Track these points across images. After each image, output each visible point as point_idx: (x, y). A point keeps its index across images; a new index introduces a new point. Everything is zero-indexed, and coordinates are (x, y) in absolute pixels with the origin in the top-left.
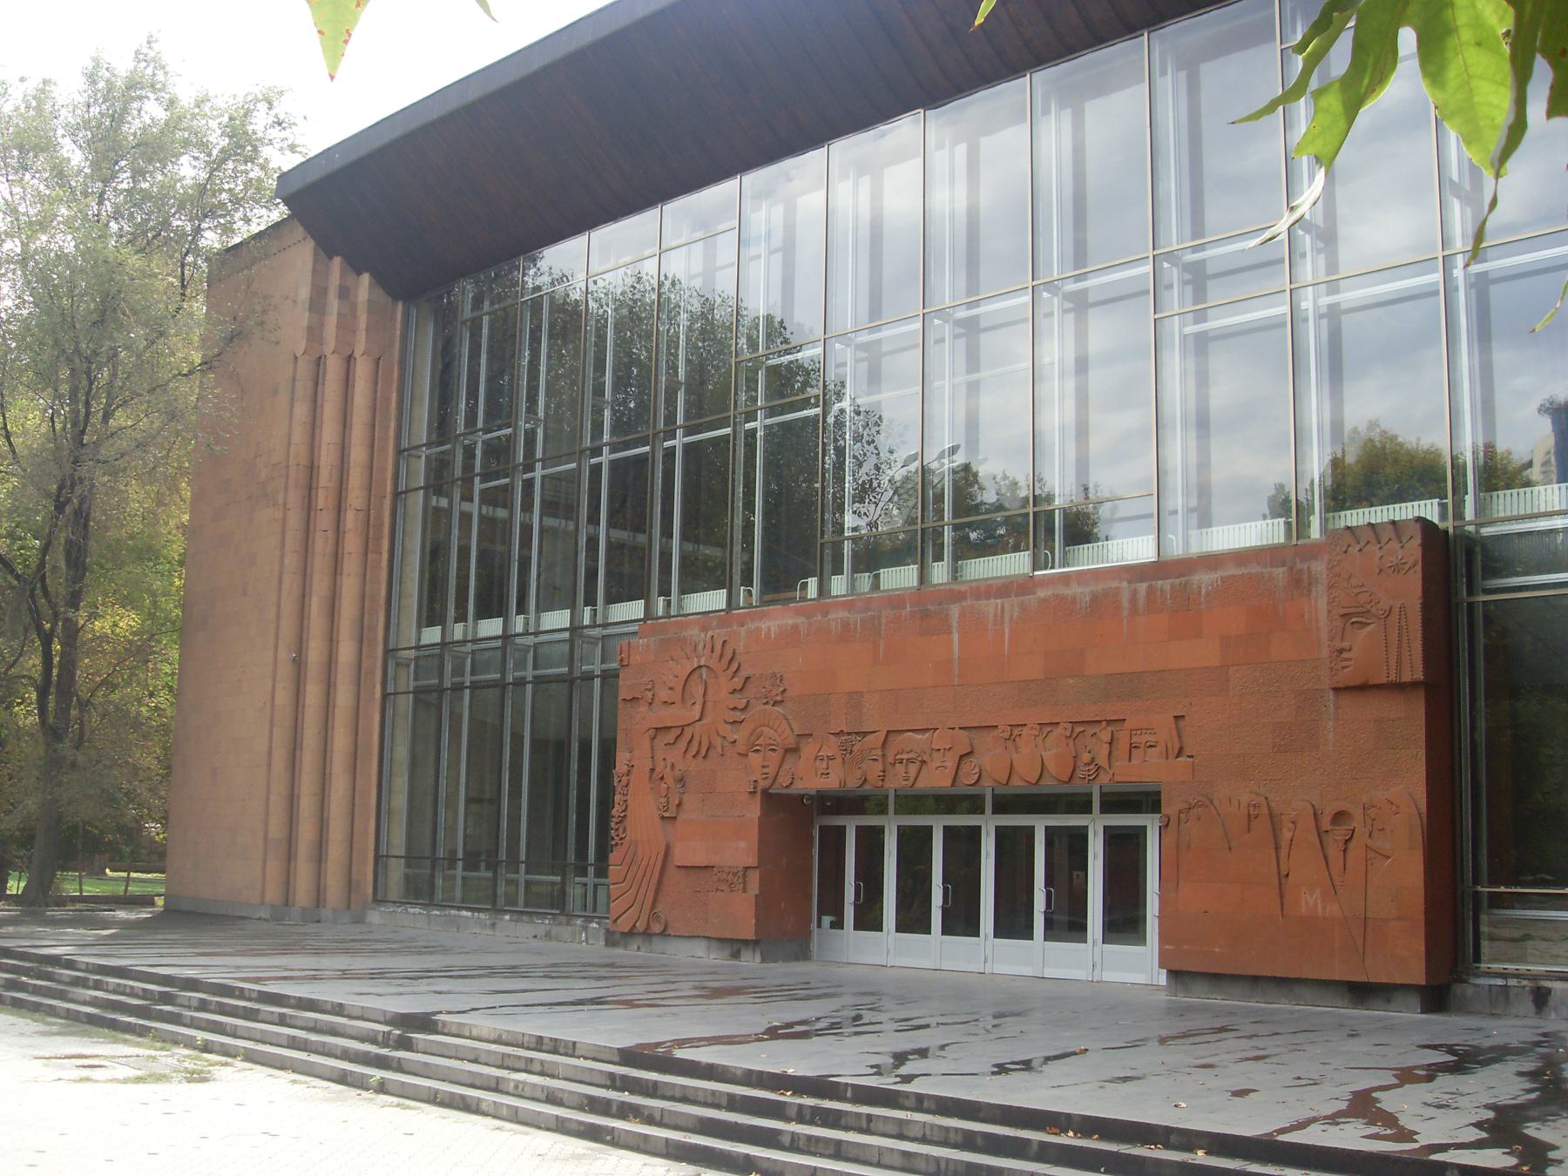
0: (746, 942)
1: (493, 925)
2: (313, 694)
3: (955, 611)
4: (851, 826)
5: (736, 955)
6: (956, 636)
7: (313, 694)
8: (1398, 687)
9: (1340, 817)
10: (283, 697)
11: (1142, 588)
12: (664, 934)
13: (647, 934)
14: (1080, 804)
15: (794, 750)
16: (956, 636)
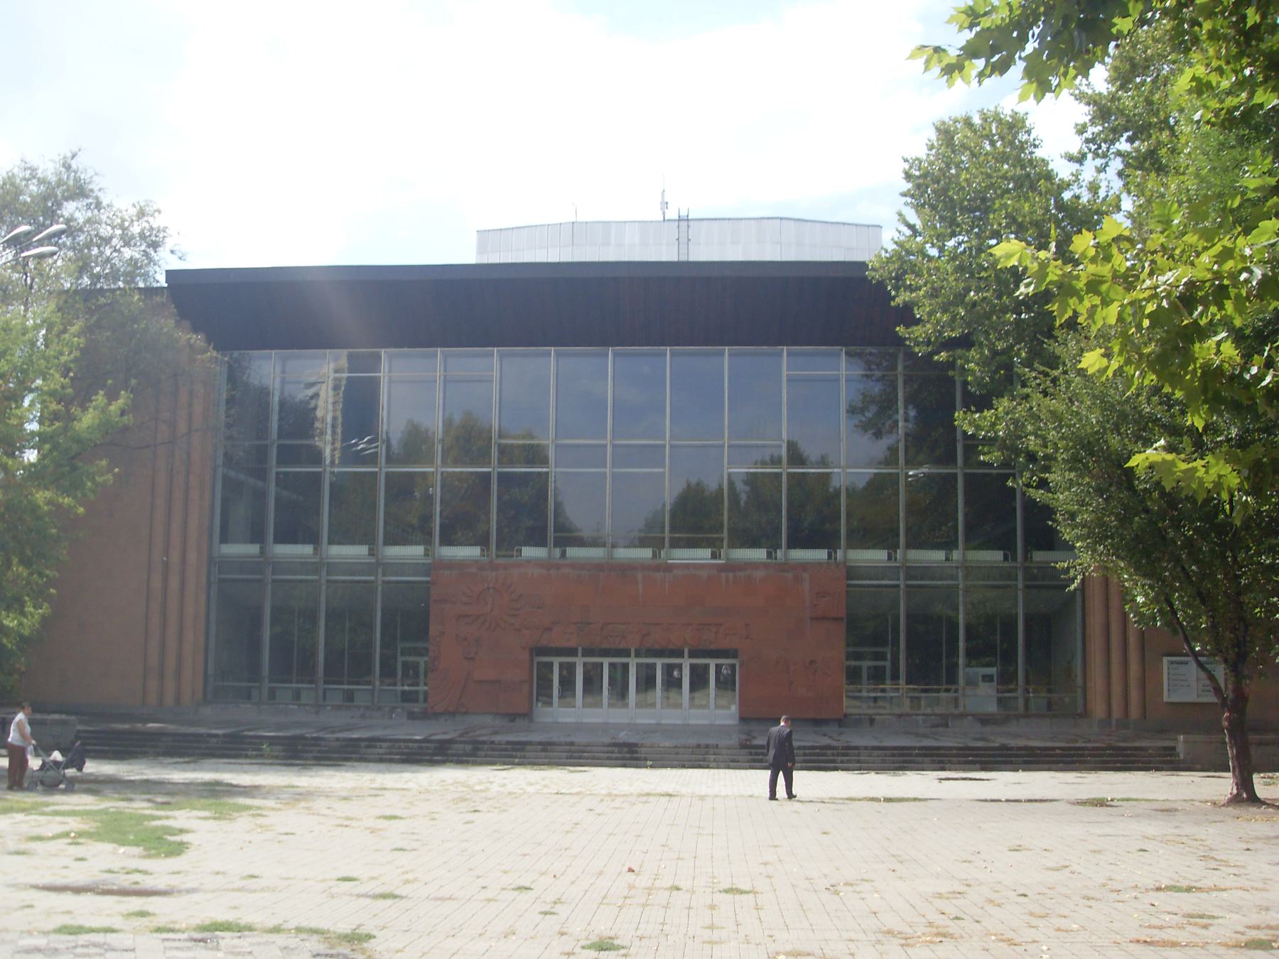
0: (520, 715)
1: (317, 713)
2: (174, 582)
3: (640, 576)
4: (556, 661)
5: (513, 721)
6: (640, 586)
7: (174, 582)
8: (835, 619)
9: (812, 662)
10: (157, 582)
11: (731, 575)
12: (466, 713)
13: (453, 714)
14: (679, 654)
15: (549, 629)
16: (640, 586)
